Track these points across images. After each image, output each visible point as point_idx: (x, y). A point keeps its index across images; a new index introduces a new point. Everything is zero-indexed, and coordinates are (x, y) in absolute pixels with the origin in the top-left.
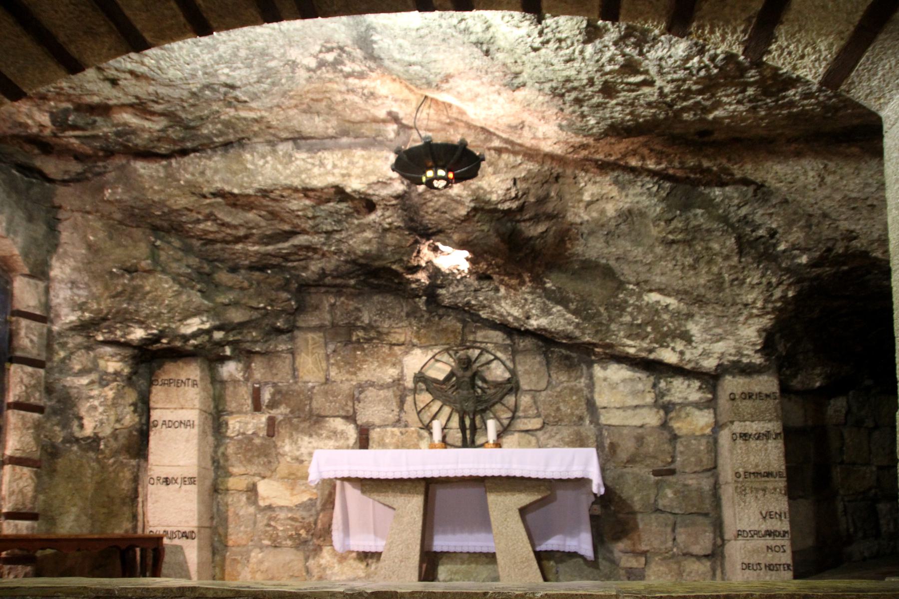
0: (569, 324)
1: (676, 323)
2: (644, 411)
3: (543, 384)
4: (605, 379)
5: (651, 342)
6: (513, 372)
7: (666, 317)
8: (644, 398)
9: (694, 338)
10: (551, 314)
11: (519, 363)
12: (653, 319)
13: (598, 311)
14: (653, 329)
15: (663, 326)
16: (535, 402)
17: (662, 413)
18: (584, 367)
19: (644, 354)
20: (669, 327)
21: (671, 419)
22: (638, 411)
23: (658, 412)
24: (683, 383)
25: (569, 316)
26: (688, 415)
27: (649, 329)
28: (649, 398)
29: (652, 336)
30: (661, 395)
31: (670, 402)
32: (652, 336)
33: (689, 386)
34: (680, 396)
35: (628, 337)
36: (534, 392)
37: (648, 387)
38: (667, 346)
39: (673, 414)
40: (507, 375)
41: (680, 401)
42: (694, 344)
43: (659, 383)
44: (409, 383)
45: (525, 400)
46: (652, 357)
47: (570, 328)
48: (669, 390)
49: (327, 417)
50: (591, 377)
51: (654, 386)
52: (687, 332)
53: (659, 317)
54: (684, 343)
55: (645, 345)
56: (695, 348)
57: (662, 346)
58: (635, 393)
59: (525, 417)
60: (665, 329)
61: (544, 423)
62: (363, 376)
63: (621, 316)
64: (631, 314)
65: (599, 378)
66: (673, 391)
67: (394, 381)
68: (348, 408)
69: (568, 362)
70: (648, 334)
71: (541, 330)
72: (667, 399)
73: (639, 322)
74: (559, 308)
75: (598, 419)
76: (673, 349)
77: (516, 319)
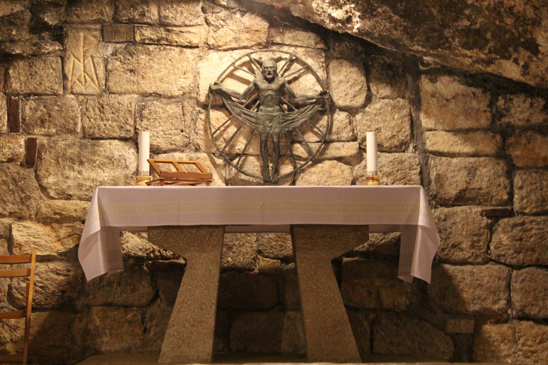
0: (395, 28)
1: (521, 29)
2: (479, 136)
3: (360, 100)
4: (433, 96)
5: (490, 52)
6: (325, 84)
7: (509, 21)
8: (478, 120)
9: (540, 48)
10: (375, 16)
11: (334, 73)
12: (494, 24)
13: (431, 14)
14: (493, 36)
15: (506, 33)
16: (350, 123)
17: (498, 138)
18: (410, 79)
19: (480, 67)
20: (512, 33)
21: (509, 146)
22: (471, 134)
23: (494, 137)
24: (524, 102)
25: (396, 18)
26: (529, 141)
27: (489, 36)
28: (484, 121)
29: (491, 44)
30: (497, 115)
31: (508, 125)
32: (491, 44)
33: (532, 105)
34: (521, 117)
35: (466, 46)
36: (351, 111)
37: (483, 106)
38: (509, 58)
39: (511, 140)
40: (319, 89)
41: (520, 124)
42: (540, 56)
43: (497, 100)
44: (202, 99)
45: (340, 117)
46: (490, 69)
47: (396, 34)
48: (508, 110)
49: (102, 138)
50: (417, 91)
51: (491, 104)
52: (534, 40)
53: (502, 21)
54: (528, 54)
55: (482, 56)
56: (541, 60)
57: (503, 57)
58: (467, 113)
59: (339, 141)
60: (507, 36)
61: (360, 148)
62: (148, 87)
63: (456, 19)
64: (469, 18)
65: (426, 93)
66: (513, 111)
67: (184, 94)
68: (128, 127)
69: (390, 73)
70: (487, 41)
71: (363, 34)
72: (505, 120)
73: (477, 26)
74: (385, 8)
75: (424, 144)
76: (516, 61)
77: (334, 20)
